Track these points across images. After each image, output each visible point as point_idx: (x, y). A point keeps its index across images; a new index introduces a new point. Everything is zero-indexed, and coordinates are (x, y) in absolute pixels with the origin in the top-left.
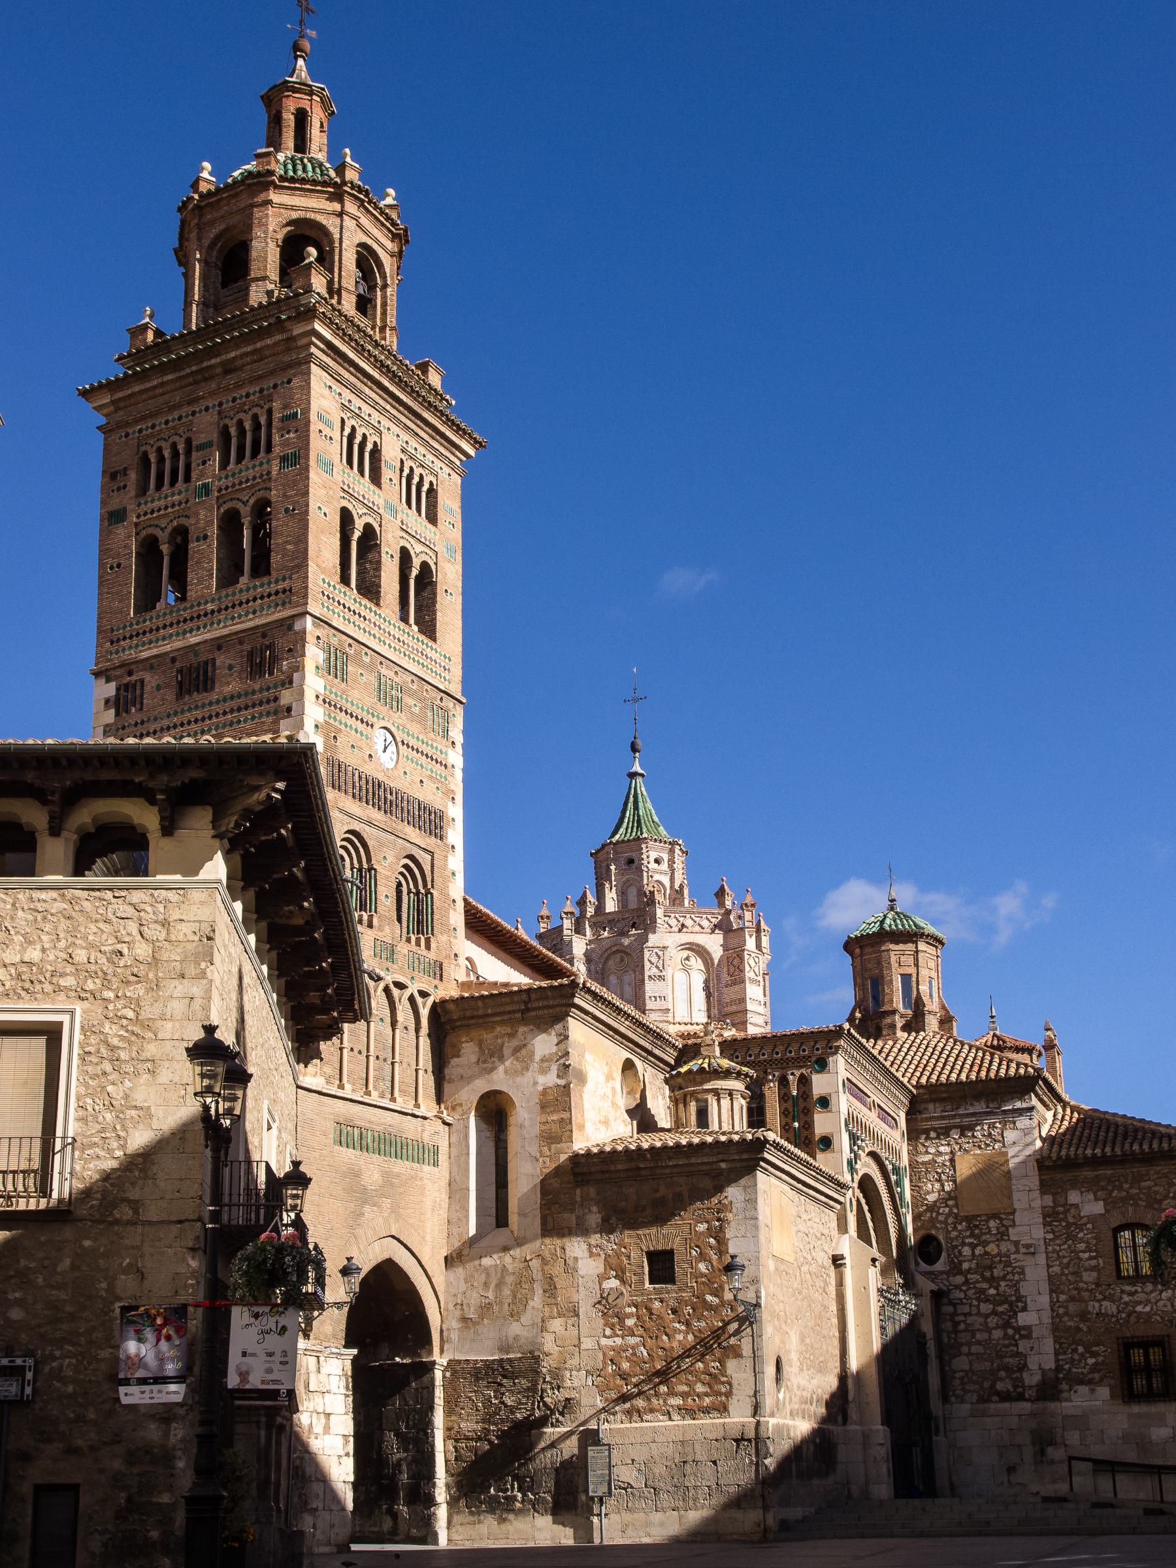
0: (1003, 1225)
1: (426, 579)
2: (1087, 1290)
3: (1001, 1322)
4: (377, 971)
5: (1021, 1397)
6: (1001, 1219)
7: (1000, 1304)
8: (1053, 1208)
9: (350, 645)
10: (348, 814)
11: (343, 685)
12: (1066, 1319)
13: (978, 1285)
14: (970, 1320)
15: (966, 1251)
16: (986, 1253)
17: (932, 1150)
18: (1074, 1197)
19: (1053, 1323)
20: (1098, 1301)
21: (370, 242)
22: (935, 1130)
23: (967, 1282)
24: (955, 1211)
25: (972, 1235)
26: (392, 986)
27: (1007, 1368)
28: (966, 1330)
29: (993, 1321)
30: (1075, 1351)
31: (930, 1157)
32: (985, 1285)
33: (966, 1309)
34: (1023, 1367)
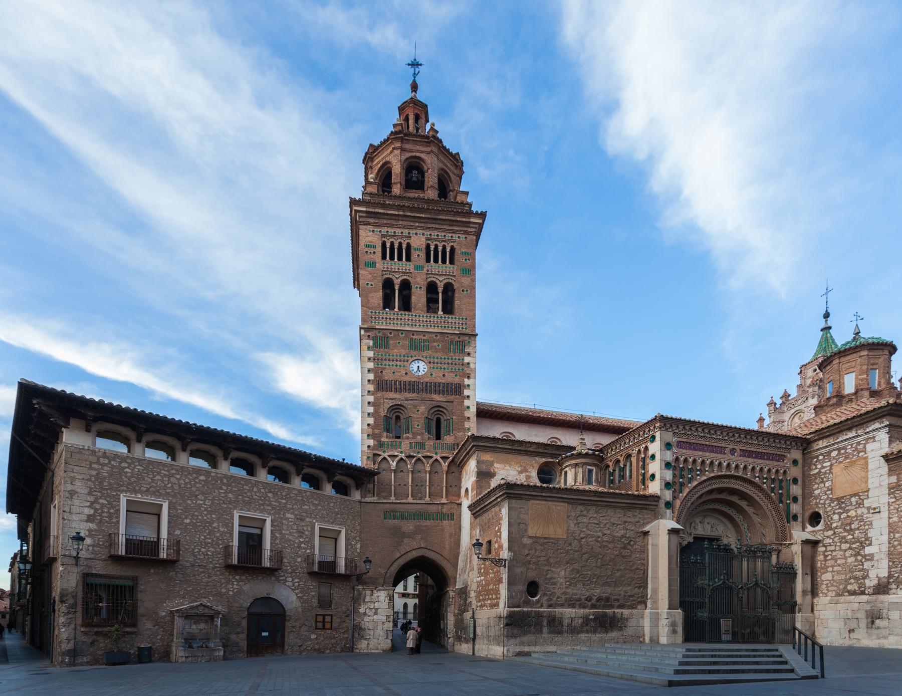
1: (449, 288)
3: (854, 553)
5: (863, 593)
9: (390, 333)
10: (392, 399)
11: (386, 350)
15: (836, 517)
24: (831, 496)
31: (817, 470)
32: (845, 534)
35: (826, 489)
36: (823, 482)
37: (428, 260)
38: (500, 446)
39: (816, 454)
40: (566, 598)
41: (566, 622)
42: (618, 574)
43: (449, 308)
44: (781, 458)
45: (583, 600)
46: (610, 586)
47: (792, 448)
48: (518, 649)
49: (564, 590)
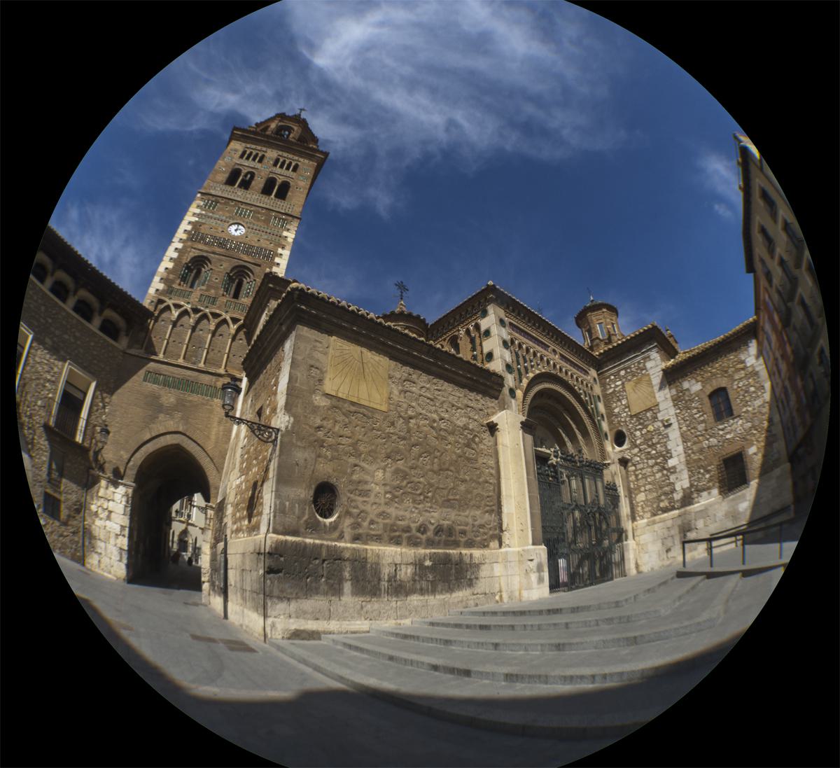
0: (654, 413)
2: (702, 435)
4: (199, 307)
5: (673, 508)
6: (652, 410)
7: (658, 459)
8: (677, 395)
10: (199, 250)
12: (692, 455)
13: (646, 451)
14: (644, 471)
16: (648, 431)
17: (613, 386)
18: (686, 385)
19: (686, 460)
20: (708, 439)
22: (612, 375)
23: (640, 450)
24: (629, 413)
25: (640, 424)
26: (209, 314)
27: (666, 494)
28: (642, 478)
29: (656, 468)
30: (699, 473)
32: (649, 450)
33: (641, 466)
34: (673, 491)
35: (623, 407)
36: (620, 400)
37: (275, 165)
39: (607, 374)
40: (385, 525)
41: (386, 571)
44: (586, 373)
45: (414, 531)
46: (452, 507)
48: (295, 625)
49: (382, 508)
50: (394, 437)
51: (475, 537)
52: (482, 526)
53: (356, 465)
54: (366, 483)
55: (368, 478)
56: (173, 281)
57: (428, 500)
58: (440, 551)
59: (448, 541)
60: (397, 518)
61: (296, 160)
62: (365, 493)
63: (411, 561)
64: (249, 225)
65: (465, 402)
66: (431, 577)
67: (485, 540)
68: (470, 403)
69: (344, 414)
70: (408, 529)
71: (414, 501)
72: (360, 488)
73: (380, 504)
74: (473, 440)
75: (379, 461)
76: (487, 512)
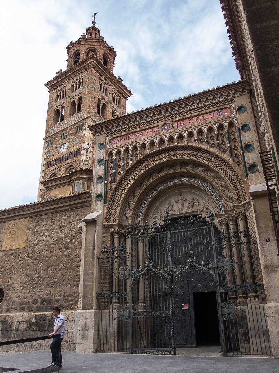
21: (76, 50)
38: (59, 183)
41: (15, 326)
42: (60, 274)
43: (79, 109)
47: (234, 97)
50: (28, 258)
51: (65, 303)
52: (69, 296)
53: (11, 277)
54: (13, 284)
55: (14, 282)
56: (44, 194)
57: (40, 285)
58: (42, 313)
59: (47, 307)
60: (24, 298)
61: (81, 77)
62: (12, 289)
63: (26, 320)
64: (67, 141)
65: (69, 220)
66: (34, 328)
67: (71, 304)
68: (72, 220)
69: (8, 256)
70: (28, 303)
71: (33, 288)
72: (11, 287)
73: (18, 293)
74: (71, 243)
75: (19, 272)
76: (75, 286)
